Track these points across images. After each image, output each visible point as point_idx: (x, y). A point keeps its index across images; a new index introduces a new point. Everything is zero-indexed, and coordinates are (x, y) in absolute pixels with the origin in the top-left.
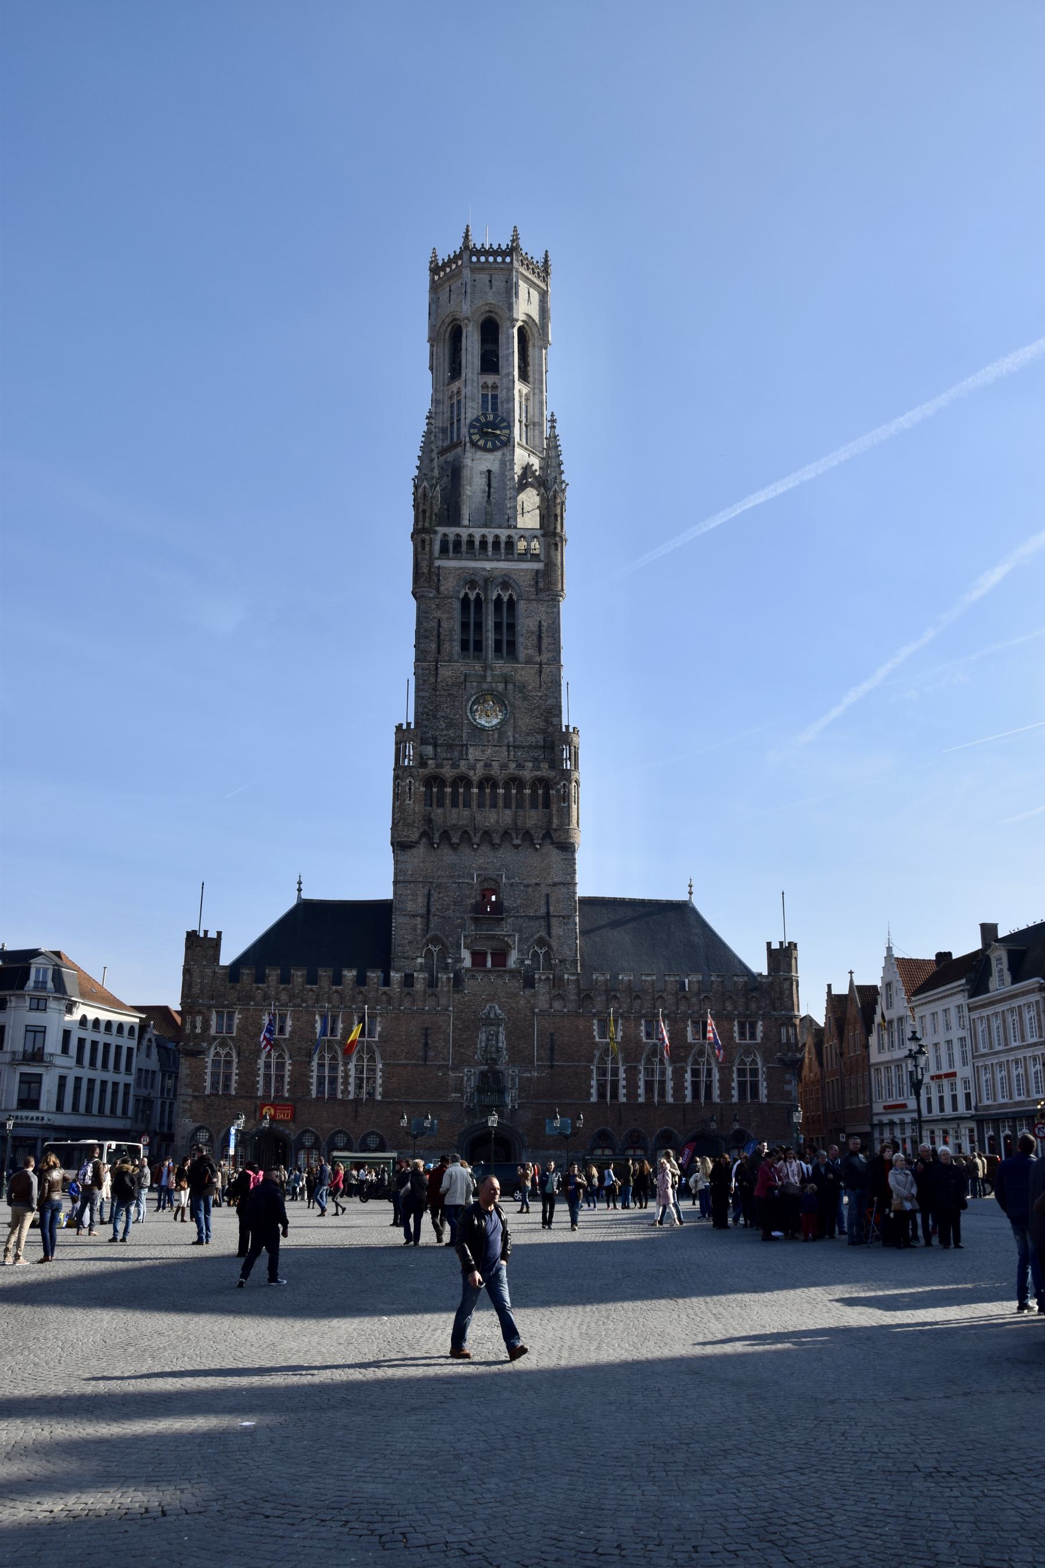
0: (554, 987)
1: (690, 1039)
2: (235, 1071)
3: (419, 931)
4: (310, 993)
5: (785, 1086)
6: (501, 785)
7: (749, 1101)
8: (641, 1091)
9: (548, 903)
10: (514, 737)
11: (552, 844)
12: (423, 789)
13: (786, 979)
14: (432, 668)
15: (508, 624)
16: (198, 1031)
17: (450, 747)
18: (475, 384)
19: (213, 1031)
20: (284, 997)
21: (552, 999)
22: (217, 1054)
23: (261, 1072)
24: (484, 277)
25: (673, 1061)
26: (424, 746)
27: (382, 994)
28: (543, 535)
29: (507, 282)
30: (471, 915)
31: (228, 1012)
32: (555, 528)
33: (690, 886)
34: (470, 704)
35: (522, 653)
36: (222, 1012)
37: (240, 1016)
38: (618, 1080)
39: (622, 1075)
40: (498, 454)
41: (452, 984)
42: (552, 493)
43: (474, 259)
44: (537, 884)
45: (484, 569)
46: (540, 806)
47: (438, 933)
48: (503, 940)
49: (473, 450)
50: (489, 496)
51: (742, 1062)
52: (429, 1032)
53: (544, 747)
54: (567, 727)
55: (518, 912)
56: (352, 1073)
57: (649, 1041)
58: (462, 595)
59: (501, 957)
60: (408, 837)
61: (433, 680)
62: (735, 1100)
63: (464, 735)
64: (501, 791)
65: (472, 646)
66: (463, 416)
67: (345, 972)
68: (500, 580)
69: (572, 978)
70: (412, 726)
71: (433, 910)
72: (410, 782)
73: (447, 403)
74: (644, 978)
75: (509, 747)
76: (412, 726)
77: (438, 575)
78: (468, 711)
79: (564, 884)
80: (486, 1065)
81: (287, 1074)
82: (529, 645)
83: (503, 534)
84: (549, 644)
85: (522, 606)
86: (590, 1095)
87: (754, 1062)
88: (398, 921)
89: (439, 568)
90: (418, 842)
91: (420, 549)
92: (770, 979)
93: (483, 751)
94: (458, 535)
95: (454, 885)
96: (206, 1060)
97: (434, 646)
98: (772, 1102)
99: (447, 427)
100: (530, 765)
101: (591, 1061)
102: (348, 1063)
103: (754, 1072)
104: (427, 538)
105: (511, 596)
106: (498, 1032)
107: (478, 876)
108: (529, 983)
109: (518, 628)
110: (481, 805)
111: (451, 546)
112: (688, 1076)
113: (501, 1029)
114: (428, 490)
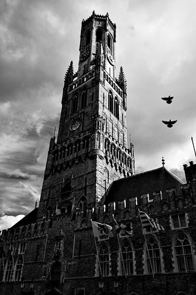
21: (82, 223)
33: (163, 160)
39: (110, 259)
44: (83, 175)
51: (178, 243)
56: (15, 269)
59: (70, 208)
62: (176, 270)
65: (74, 111)
67: (20, 227)
80: (55, 260)
86: (94, 273)
87: (186, 242)
110: (68, 155)
112: (144, 256)
113: (62, 241)
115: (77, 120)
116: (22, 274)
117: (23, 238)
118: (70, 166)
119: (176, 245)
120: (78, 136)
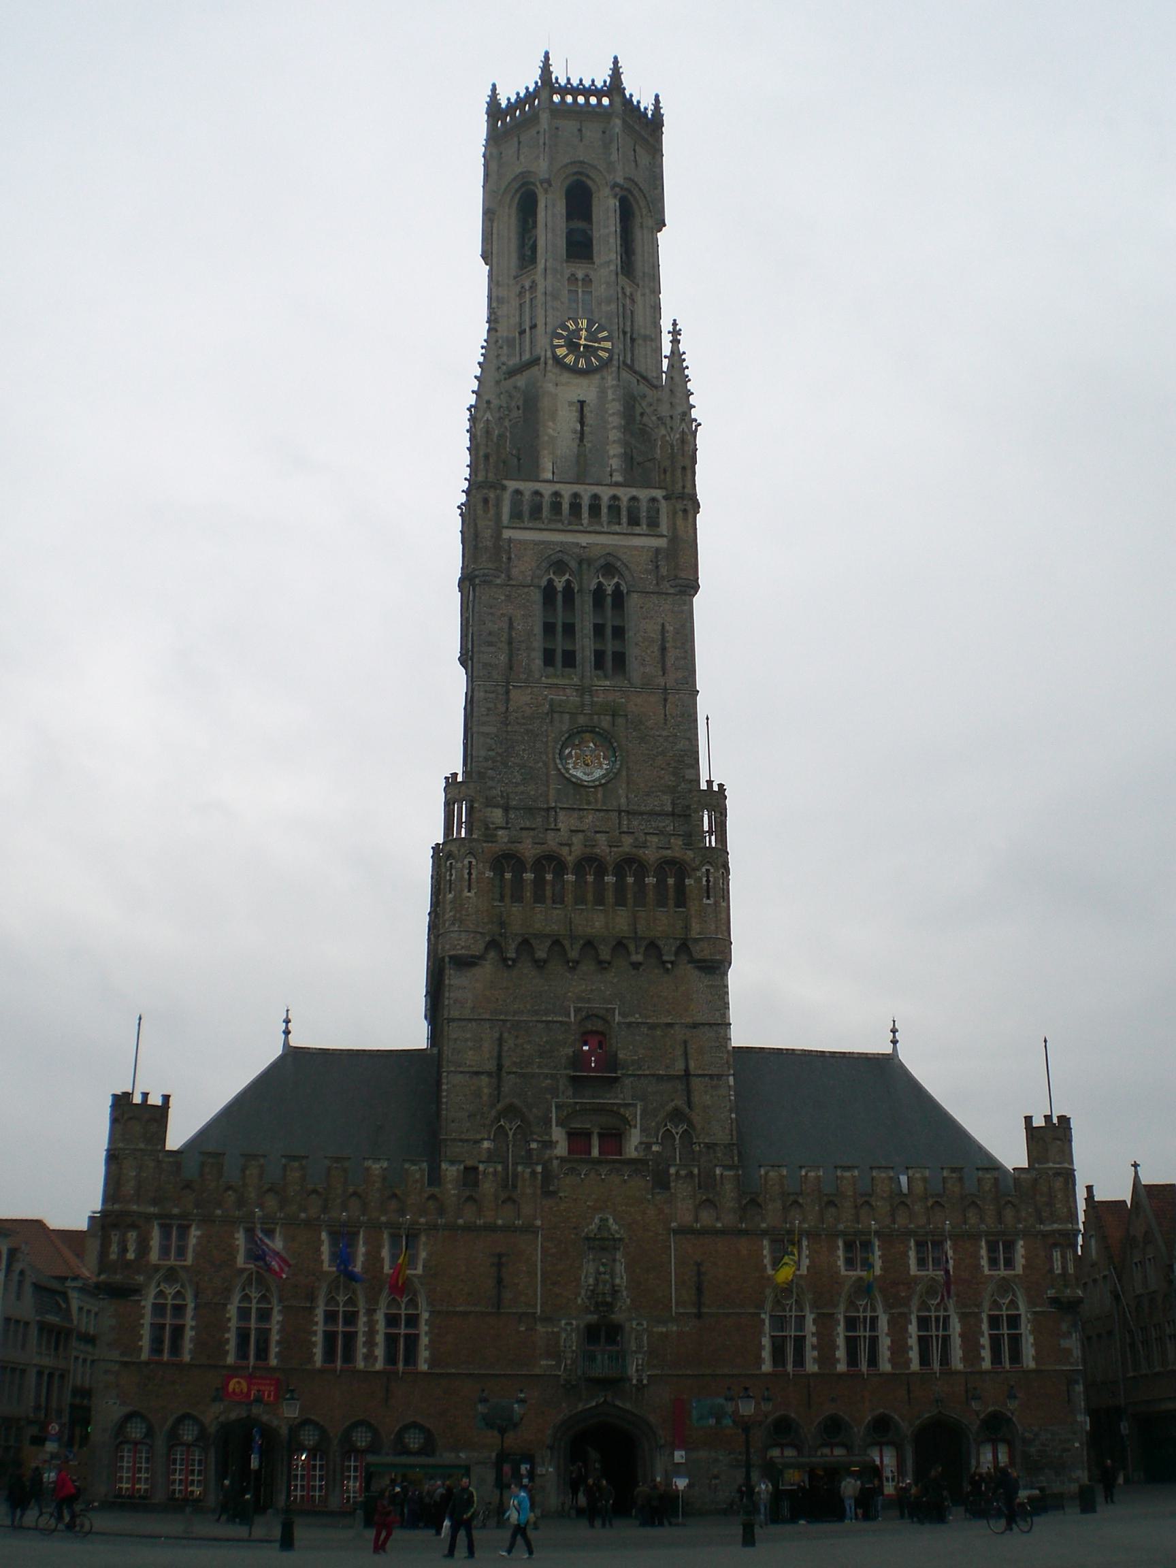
0: (700, 1188)
1: (913, 1270)
2: (189, 1321)
3: (485, 1098)
4: (314, 1196)
5: (1062, 1342)
6: (610, 869)
7: (1008, 1366)
8: (841, 1353)
9: (686, 1054)
10: (627, 797)
11: (689, 962)
12: (491, 874)
13: (1058, 1173)
14: (501, 690)
15: (614, 627)
16: (131, 1256)
17: (530, 811)
18: (559, 277)
19: (154, 1256)
20: (271, 1202)
22: (161, 1294)
23: (233, 1324)
24: (570, 126)
25: (888, 1306)
26: (489, 809)
27: (429, 1198)
28: (666, 498)
29: (604, 132)
30: (568, 1072)
31: (180, 1227)
32: (684, 487)
33: (894, 1031)
34: (559, 747)
35: (635, 668)
36: (170, 1226)
37: (198, 1233)
38: (805, 1336)
39: (810, 1327)
40: (596, 378)
41: (539, 1182)
42: (678, 436)
43: (556, 98)
44: (670, 1025)
45: (577, 544)
46: (671, 902)
47: (516, 1101)
48: (619, 1113)
49: (556, 370)
50: (581, 439)
51: (996, 1305)
52: (504, 1259)
53: (673, 814)
54: (710, 783)
55: (640, 1068)
56: (381, 1326)
57: (851, 1273)
58: (544, 583)
59: (614, 1137)
60: (468, 948)
61: (503, 709)
62: (987, 1365)
63: (552, 793)
64: (610, 879)
66: (540, 322)
68: (602, 562)
69: (726, 1173)
71: (507, 1063)
72: (470, 863)
73: (515, 303)
74: (839, 1173)
75: (620, 812)
77: (510, 553)
78: (557, 756)
79: (710, 1025)
81: (275, 1328)
82: (648, 659)
83: (605, 493)
84: (677, 658)
85: (634, 601)
86: (759, 1361)
87: (1013, 1303)
88: (452, 1082)
89: (510, 540)
90: (482, 957)
91: (480, 512)
92: (1034, 1174)
93: (581, 818)
94: (537, 493)
95: (541, 1026)
96: (143, 1303)
97: (503, 658)
98: (1043, 1368)
99: (514, 339)
100: (655, 839)
101: (760, 1306)
102: (375, 1310)
103: (1014, 1321)
104: (492, 495)
105: (617, 585)
106: (614, 1260)
107: (577, 1010)
108: (662, 1182)
109: (630, 634)
110: (580, 900)
111: (526, 508)
113: (618, 1256)
115: (592, 730)
116: (431, 1346)
117: (402, 1212)
118: (600, 962)
119: (990, 1310)
120: (628, 840)
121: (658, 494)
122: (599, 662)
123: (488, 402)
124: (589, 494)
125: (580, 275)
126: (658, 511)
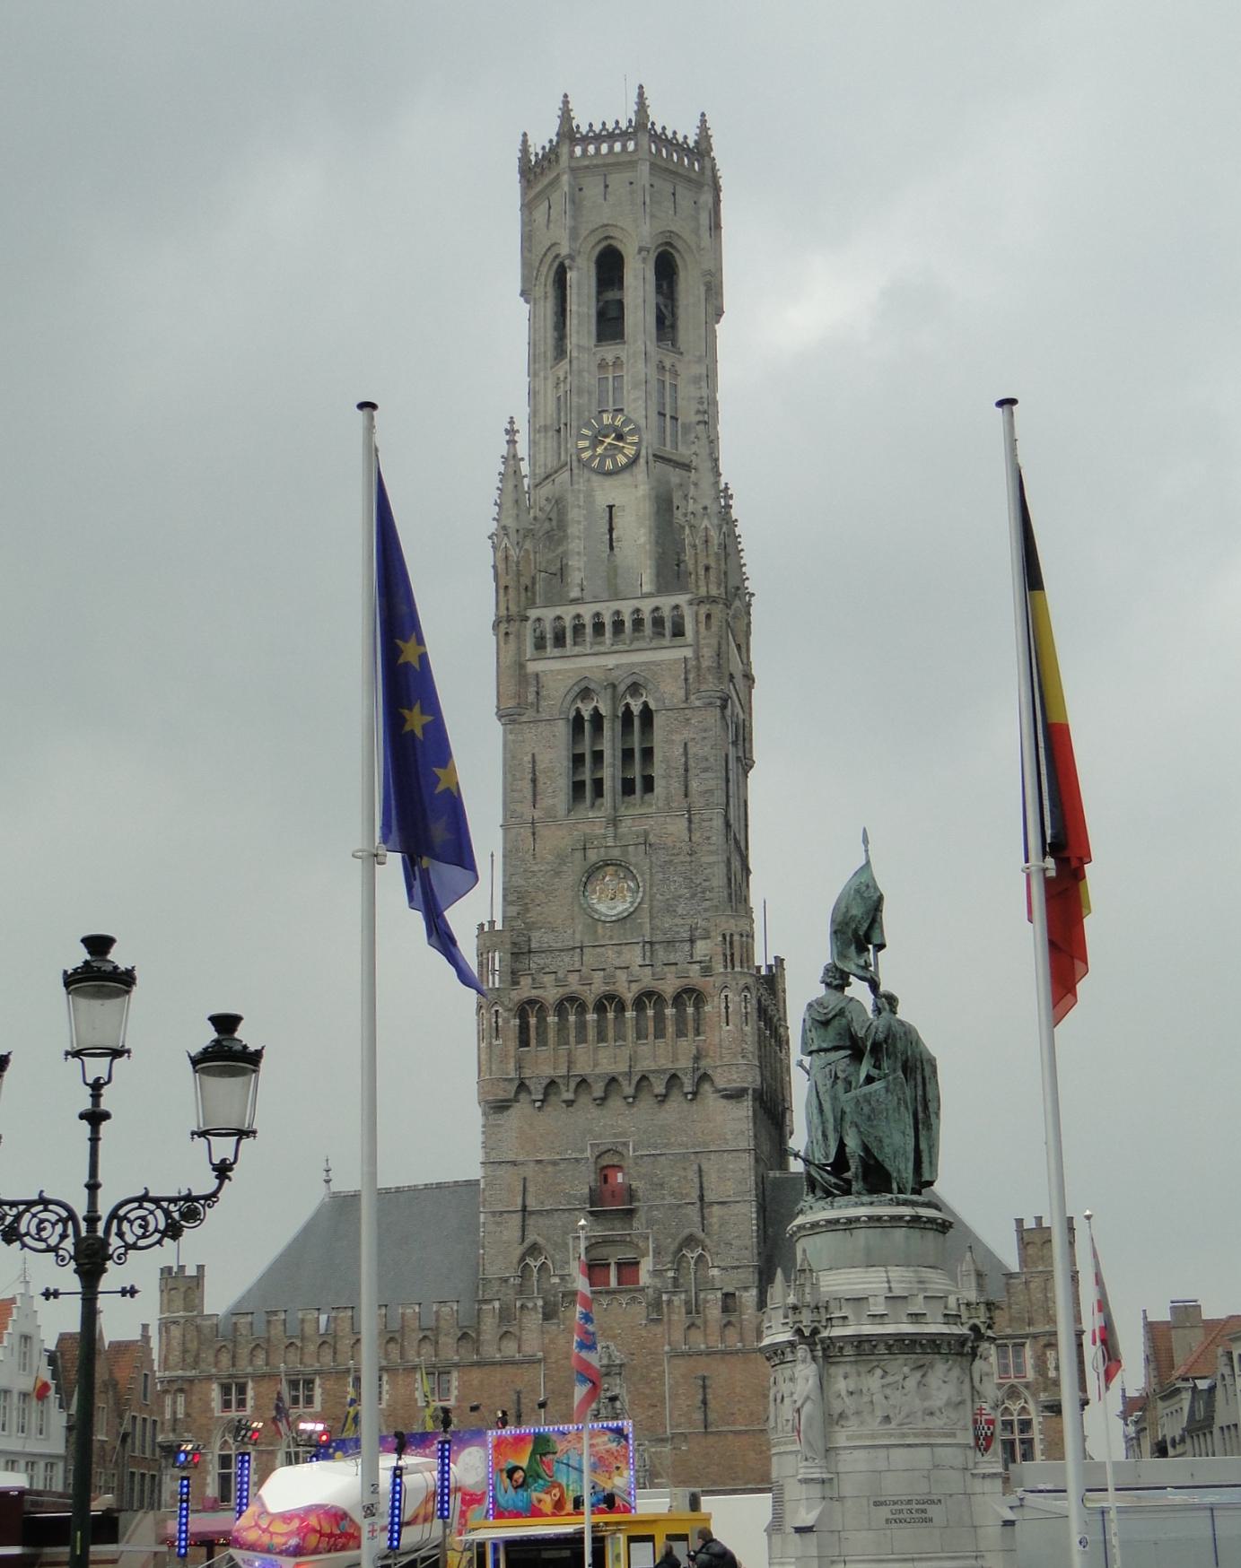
6: (629, 1003)
28: (690, 603)
43: (578, 150)
58: (572, 714)
64: (630, 1014)
68: (629, 681)
70: (498, 926)
72: (497, 1011)
76: (498, 926)
91: (502, 644)
105: (646, 704)
111: (549, 636)
114: (512, 552)
121: (682, 599)
122: (628, 787)
123: (504, 528)
124: (611, 612)
125: (610, 359)
126: (682, 617)
